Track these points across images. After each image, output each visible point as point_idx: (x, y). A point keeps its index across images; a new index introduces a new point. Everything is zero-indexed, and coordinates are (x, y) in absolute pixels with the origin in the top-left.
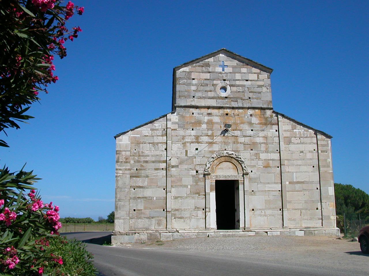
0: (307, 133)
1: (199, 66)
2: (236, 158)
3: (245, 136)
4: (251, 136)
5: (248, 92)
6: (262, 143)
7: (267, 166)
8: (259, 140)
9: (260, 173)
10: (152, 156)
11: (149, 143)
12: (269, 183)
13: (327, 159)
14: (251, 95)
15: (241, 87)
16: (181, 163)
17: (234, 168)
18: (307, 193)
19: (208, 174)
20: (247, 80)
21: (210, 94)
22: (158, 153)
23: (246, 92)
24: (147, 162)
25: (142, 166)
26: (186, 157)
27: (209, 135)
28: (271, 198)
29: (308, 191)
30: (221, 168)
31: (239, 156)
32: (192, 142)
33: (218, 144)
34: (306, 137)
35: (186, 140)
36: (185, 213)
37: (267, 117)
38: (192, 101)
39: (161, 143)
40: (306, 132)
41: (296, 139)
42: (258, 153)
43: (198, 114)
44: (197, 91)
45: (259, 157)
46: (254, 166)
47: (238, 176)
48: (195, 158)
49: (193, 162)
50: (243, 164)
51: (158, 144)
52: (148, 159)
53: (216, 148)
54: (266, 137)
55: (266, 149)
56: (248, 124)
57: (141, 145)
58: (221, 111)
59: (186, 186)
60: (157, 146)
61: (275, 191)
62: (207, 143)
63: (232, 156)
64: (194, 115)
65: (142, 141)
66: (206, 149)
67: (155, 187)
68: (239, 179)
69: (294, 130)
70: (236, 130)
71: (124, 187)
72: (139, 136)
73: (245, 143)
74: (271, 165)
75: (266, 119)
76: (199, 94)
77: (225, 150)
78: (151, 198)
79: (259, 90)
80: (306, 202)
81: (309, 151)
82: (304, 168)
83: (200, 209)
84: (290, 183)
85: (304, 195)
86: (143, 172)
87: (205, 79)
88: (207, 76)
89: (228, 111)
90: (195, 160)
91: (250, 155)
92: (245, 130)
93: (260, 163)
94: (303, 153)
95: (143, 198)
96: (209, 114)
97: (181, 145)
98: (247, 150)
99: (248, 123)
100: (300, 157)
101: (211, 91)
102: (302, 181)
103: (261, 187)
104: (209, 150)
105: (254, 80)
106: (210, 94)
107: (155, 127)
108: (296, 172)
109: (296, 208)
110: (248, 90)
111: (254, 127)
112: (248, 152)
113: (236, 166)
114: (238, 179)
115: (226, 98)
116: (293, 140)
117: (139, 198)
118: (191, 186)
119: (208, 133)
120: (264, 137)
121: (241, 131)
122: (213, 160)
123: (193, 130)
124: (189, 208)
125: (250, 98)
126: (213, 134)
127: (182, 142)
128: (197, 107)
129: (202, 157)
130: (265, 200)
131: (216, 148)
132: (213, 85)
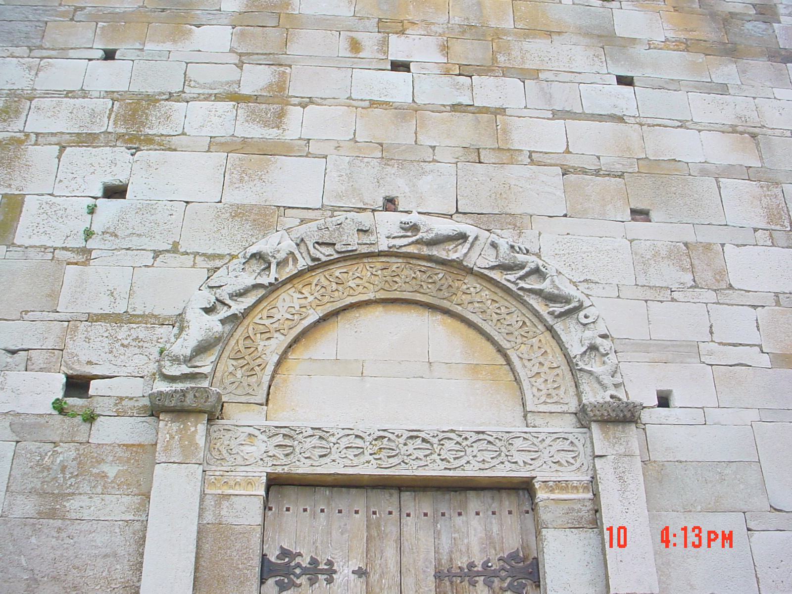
2: (495, 275)
4: (621, 119)
6: (729, 171)
17: (475, 369)
19: (189, 401)
31: (521, 258)
32: (86, 140)
33: (325, 157)
35: (36, 123)
42: (708, 247)
45: (722, 274)
47: (518, 443)
48: (80, 258)
49: (54, 296)
50: (571, 322)
62: (214, 144)
63: (453, 256)
68: (541, 474)
70: (485, 70)
73: (572, 161)
77: (390, 204)
99: (587, 34)
113: (505, 344)
114: (524, 474)
120: (734, 130)
122: (265, 280)
123: (109, 55)
129: (157, 254)
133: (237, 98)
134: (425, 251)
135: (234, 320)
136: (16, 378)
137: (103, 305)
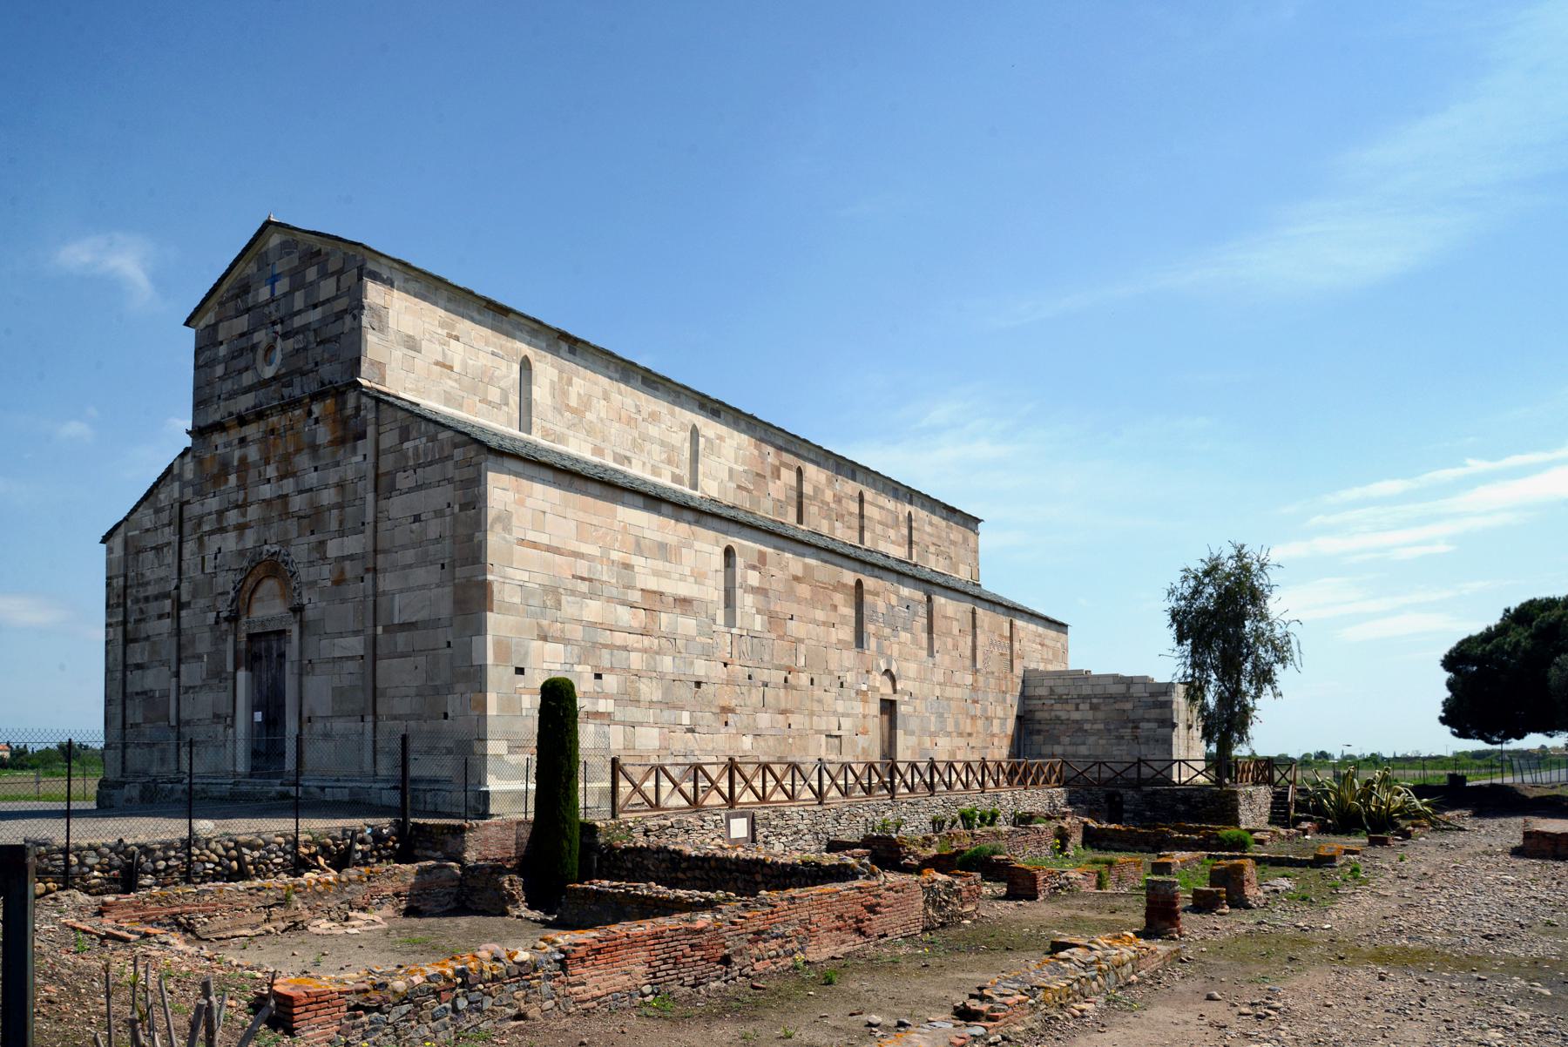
0: (433, 446)
3: (301, 492)
7: (339, 582)
8: (328, 497)
9: (324, 603)
12: (341, 635)
13: (473, 534)
18: (421, 660)
24: (147, 599)
25: (142, 611)
27: (240, 503)
34: (430, 464)
37: (348, 417)
41: (407, 474)
45: (325, 552)
46: (315, 583)
53: (250, 540)
54: (341, 486)
61: (352, 658)
67: (157, 664)
69: (406, 445)
72: (137, 532)
73: (301, 513)
81: (435, 511)
82: (421, 575)
84: (385, 628)
86: (142, 625)
94: (420, 521)
98: (305, 535)
99: (309, 447)
100: (412, 535)
102: (414, 620)
104: (240, 547)
108: (401, 591)
116: (403, 480)
117: (137, 694)
118: (208, 654)
126: (245, 499)
130: (333, 689)
133: (238, 506)
137: (220, 590)
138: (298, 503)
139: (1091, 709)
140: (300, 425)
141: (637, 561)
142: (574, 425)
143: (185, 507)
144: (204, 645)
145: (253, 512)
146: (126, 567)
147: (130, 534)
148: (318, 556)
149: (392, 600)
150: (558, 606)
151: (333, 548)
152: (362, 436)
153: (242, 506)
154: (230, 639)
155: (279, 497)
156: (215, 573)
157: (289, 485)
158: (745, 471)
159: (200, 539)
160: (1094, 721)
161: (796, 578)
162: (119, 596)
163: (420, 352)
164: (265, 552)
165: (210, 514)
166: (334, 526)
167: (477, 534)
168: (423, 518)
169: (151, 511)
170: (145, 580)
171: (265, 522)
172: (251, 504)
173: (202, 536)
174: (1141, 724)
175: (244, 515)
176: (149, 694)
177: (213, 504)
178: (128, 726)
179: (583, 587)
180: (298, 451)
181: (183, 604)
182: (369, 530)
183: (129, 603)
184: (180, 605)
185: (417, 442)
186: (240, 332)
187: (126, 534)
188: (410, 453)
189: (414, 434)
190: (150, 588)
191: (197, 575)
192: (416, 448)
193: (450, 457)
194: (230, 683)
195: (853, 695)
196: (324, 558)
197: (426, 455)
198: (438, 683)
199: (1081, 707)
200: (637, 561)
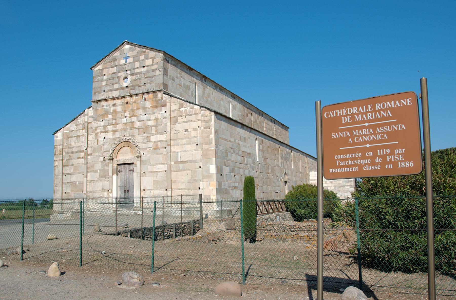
0: (192, 110)
1: (109, 62)
3: (139, 121)
5: (144, 78)
6: (153, 126)
8: (150, 123)
9: (150, 155)
10: (76, 147)
11: (75, 137)
12: (157, 164)
13: (209, 136)
14: (146, 80)
15: (139, 74)
16: (94, 151)
18: (190, 172)
20: (144, 67)
21: (116, 86)
22: (80, 144)
23: (143, 78)
24: (72, 153)
25: (70, 156)
26: (97, 146)
27: (113, 124)
28: (159, 178)
29: (191, 170)
30: (122, 153)
31: (133, 141)
34: (191, 115)
35: (99, 131)
36: (96, 194)
37: (158, 100)
38: (103, 95)
39: (82, 135)
40: (191, 109)
41: (182, 117)
42: (149, 136)
43: (107, 106)
44: (107, 85)
45: (150, 139)
46: (146, 149)
51: (79, 136)
52: (74, 150)
53: (118, 135)
54: (156, 120)
55: (156, 131)
56: (142, 109)
57: (70, 139)
58: (123, 101)
59: (96, 171)
60: (79, 138)
64: (104, 108)
65: (70, 135)
66: (111, 137)
67: (77, 173)
69: (181, 109)
71: (59, 175)
72: (68, 131)
73: (139, 128)
74: (159, 147)
75: (157, 101)
76: (108, 88)
77: (125, 136)
78: (75, 183)
79: (153, 74)
80: (189, 182)
81: (194, 129)
82: (188, 147)
83: (106, 191)
84: (175, 163)
85: (188, 174)
86: (70, 161)
87: (113, 73)
88: (114, 70)
89: (128, 99)
90: (103, 148)
91: (143, 138)
92: (140, 115)
93: (150, 145)
94: (188, 131)
95: (70, 182)
96: (114, 105)
97: (94, 135)
98: (141, 134)
99: (142, 108)
100: (185, 135)
101: (116, 83)
102: (186, 160)
103: (151, 168)
104: (114, 137)
105: (149, 66)
106: (116, 86)
107: (79, 122)
108: (181, 152)
109: (180, 187)
110: (144, 76)
111: (147, 112)
112: (142, 135)
115: (127, 87)
116: (180, 119)
117: (68, 183)
118: (100, 170)
119: (112, 123)
120: (154, 120)
121: (137, 116)
122: (115, 146)
124: (99, 190)
125: (145, 83)
126: (116, 122)
127: (95, 133)
128: (105, 100)
130: (154, 181)
131: (118, 135)
132: (119, 77)
133: (112, 125)
134: (127, 141)
135: (114, 151)
136: (101, 158)
138: (137, 124)
139: (330, 183)
140: (139, 101)
141: (240, 143)
142: (206, 102)
143: (89, 124)
144: (98, 166)
145: (119, 127)
146: (63, 142)
147: (64, 132)
148: (147, 141)
149: (177, 154)
150: (227, 156)
151: (153, 138)
152: (165, 105)
153: (115, 124)
154: (110, 165)
155: (130, 122)
156: (103, 145)
157: (134, 119)
158: (241, 115)
159: (96, 134)
160: (331, 187)
161: (268, 147)
162: (60, 152)
163: (175, 81)
164: (124, 139)
165: (100, 126)
166: (153, 131)
167: (210, 136)
168: (189, 130)
169: (75, 125)
170: (72, 146)
171: (125, 130)
172: (118, 124)
173: (97, 133)
174: (345, 187)
175: (116, 127)
176: (73, 183)
177: (102, 124)
178: (64, 193)
179: (232, 151)
180: (138, 109)
181: (89, 154)
182: (168, 133)
183: (64, 154)
184: (88, 155)
185: (186, 108)
186: (113, 72)
187: (63, 132)
188: (183, 111)
189: (185, 106)
190: (74, 149)
191: (95, 145)
192: (186, 110)
193: (200, 113)
194: (110, 179)
195: (280, 180)
196: (150, 141)
197: (189, 112)
198: (196, 179)
199: (327, 182)
200: (240, 143)
